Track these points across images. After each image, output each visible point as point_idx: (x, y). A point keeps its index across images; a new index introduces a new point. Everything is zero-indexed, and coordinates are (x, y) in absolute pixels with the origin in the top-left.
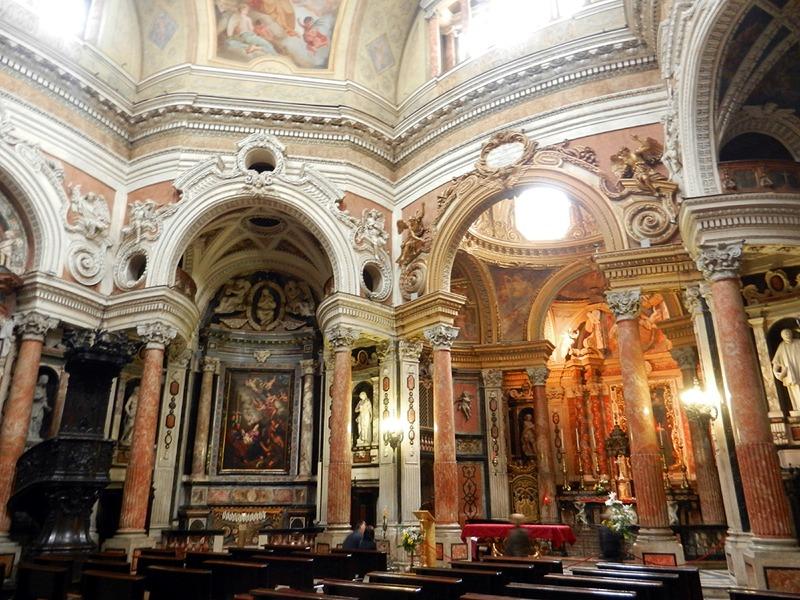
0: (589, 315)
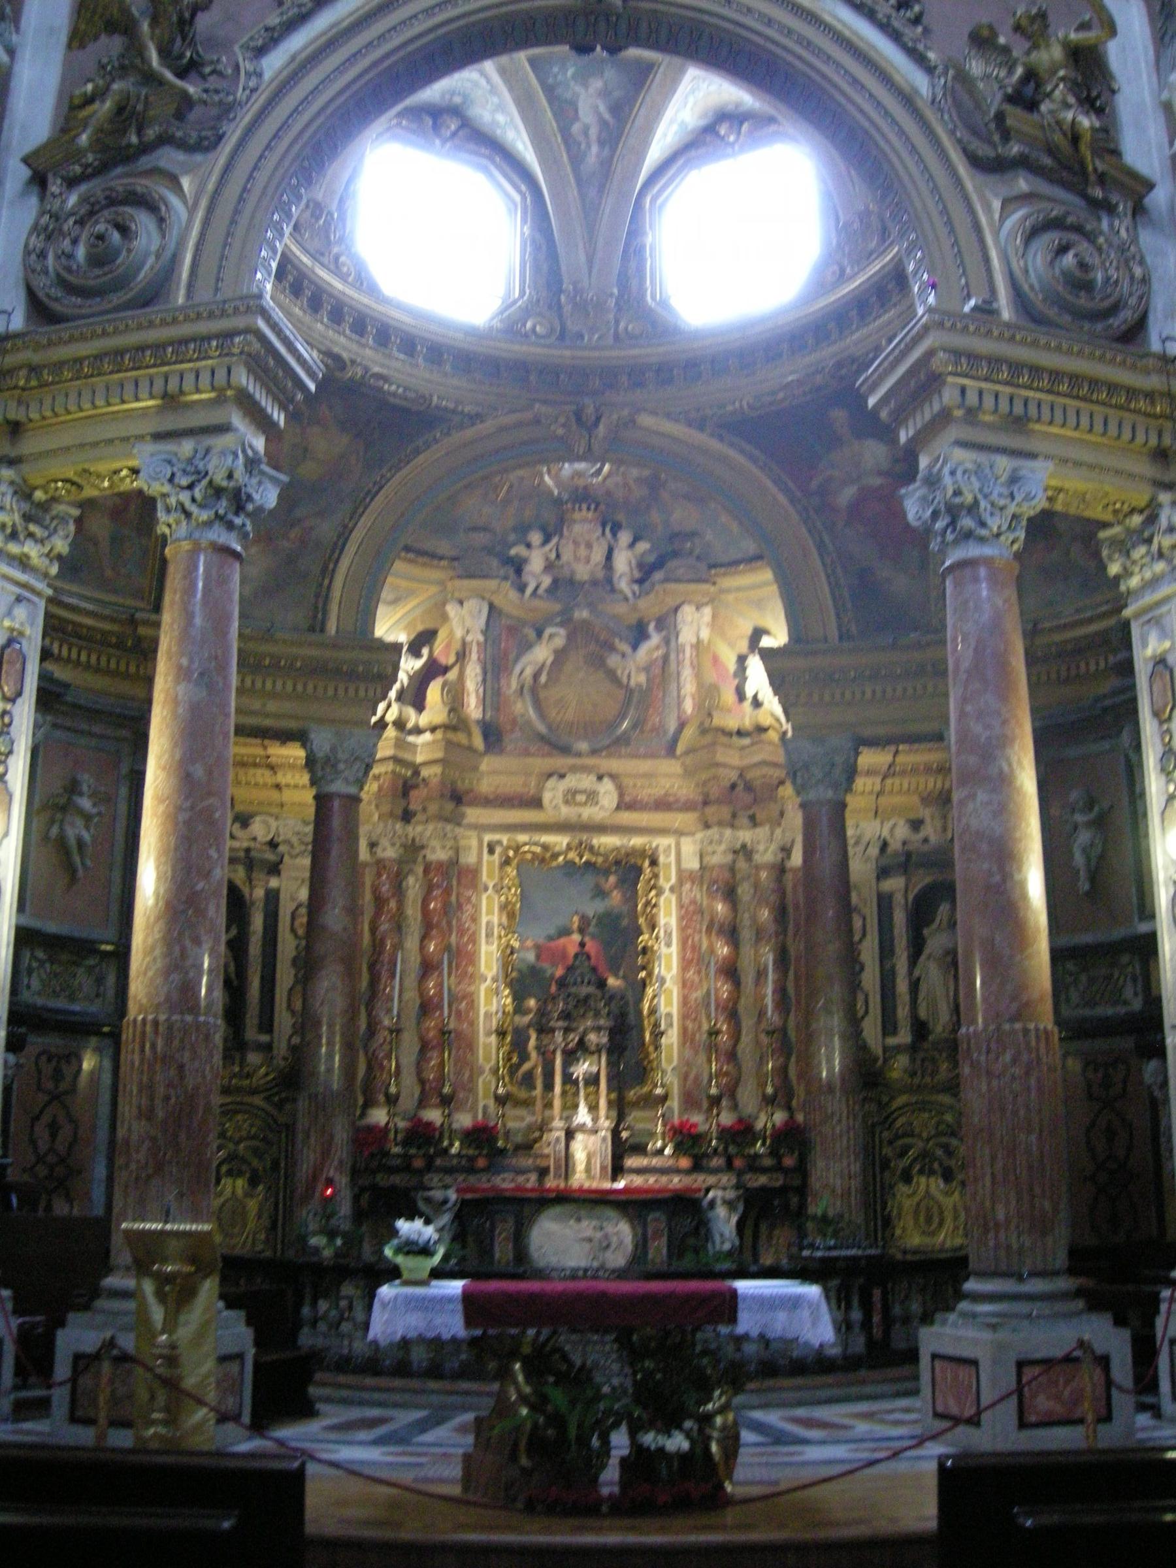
0: (452, 609)
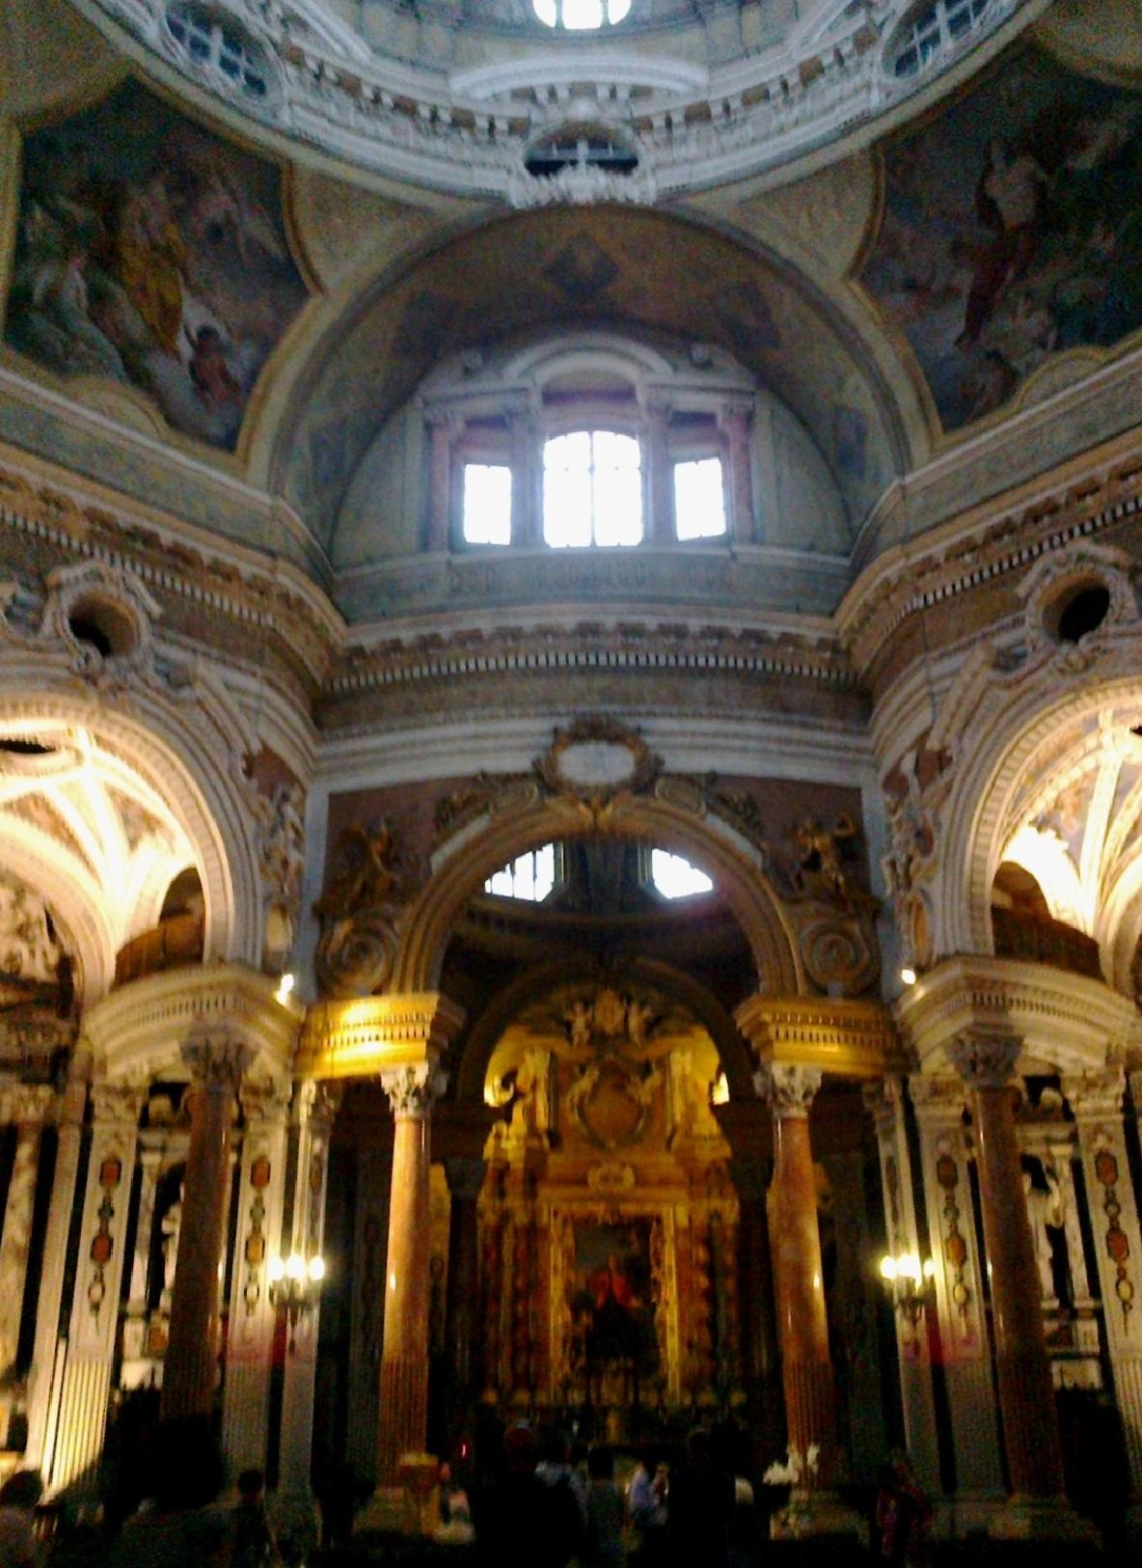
0: (528, 1057)
